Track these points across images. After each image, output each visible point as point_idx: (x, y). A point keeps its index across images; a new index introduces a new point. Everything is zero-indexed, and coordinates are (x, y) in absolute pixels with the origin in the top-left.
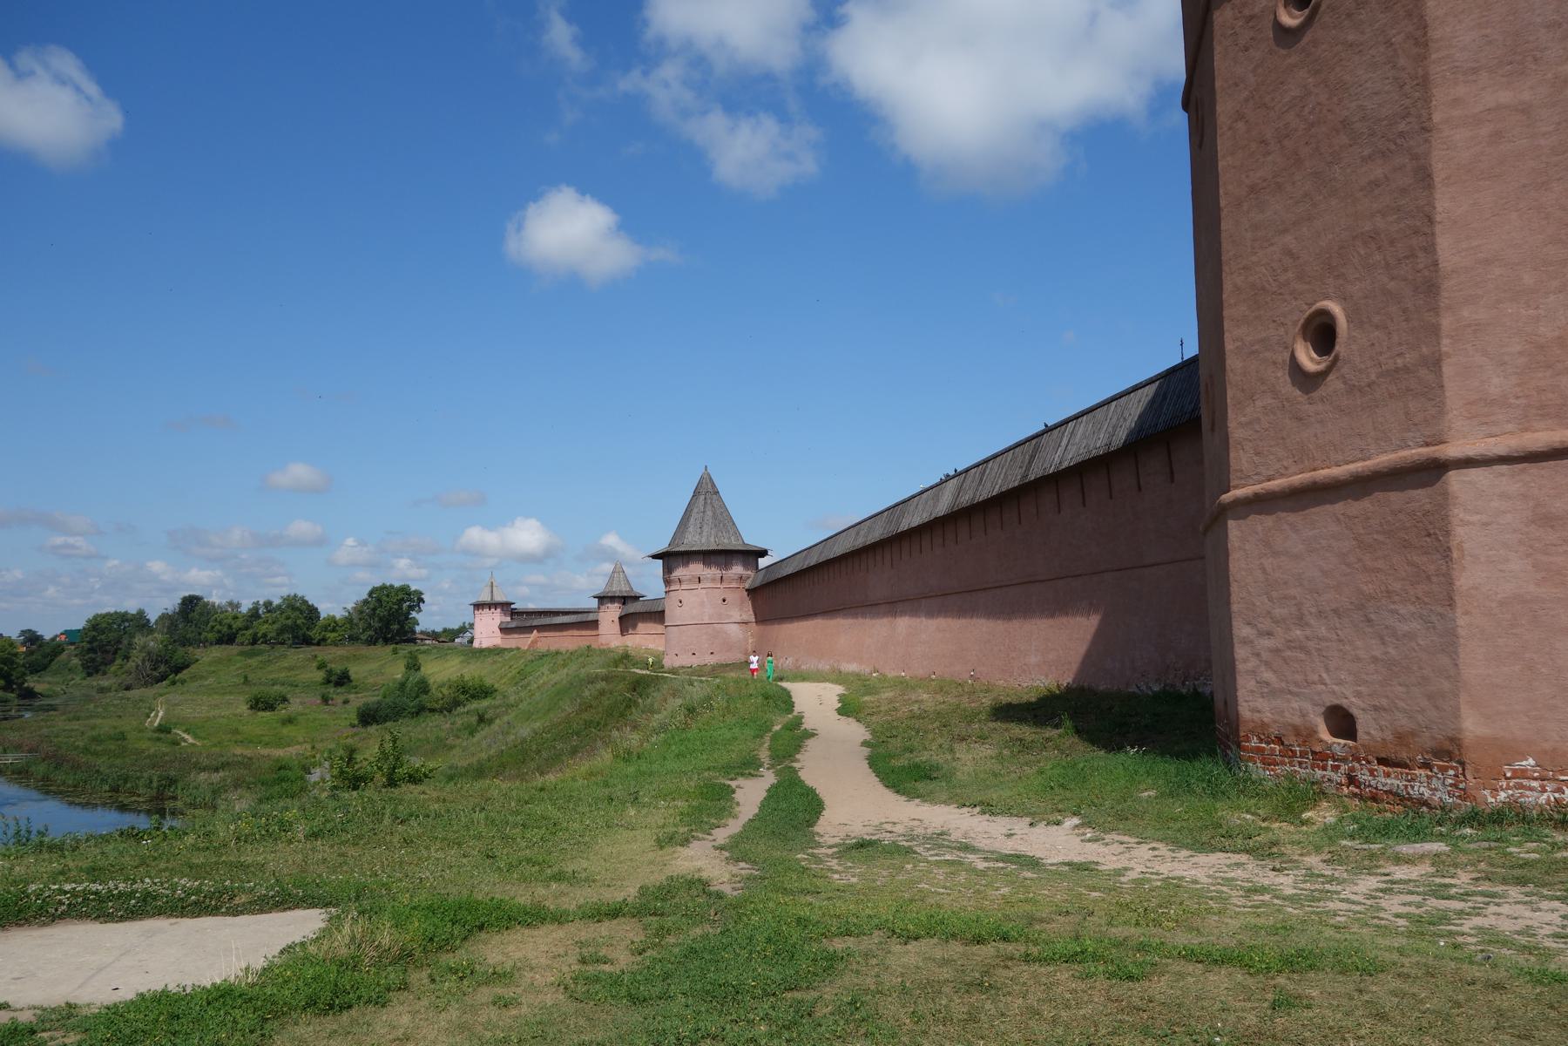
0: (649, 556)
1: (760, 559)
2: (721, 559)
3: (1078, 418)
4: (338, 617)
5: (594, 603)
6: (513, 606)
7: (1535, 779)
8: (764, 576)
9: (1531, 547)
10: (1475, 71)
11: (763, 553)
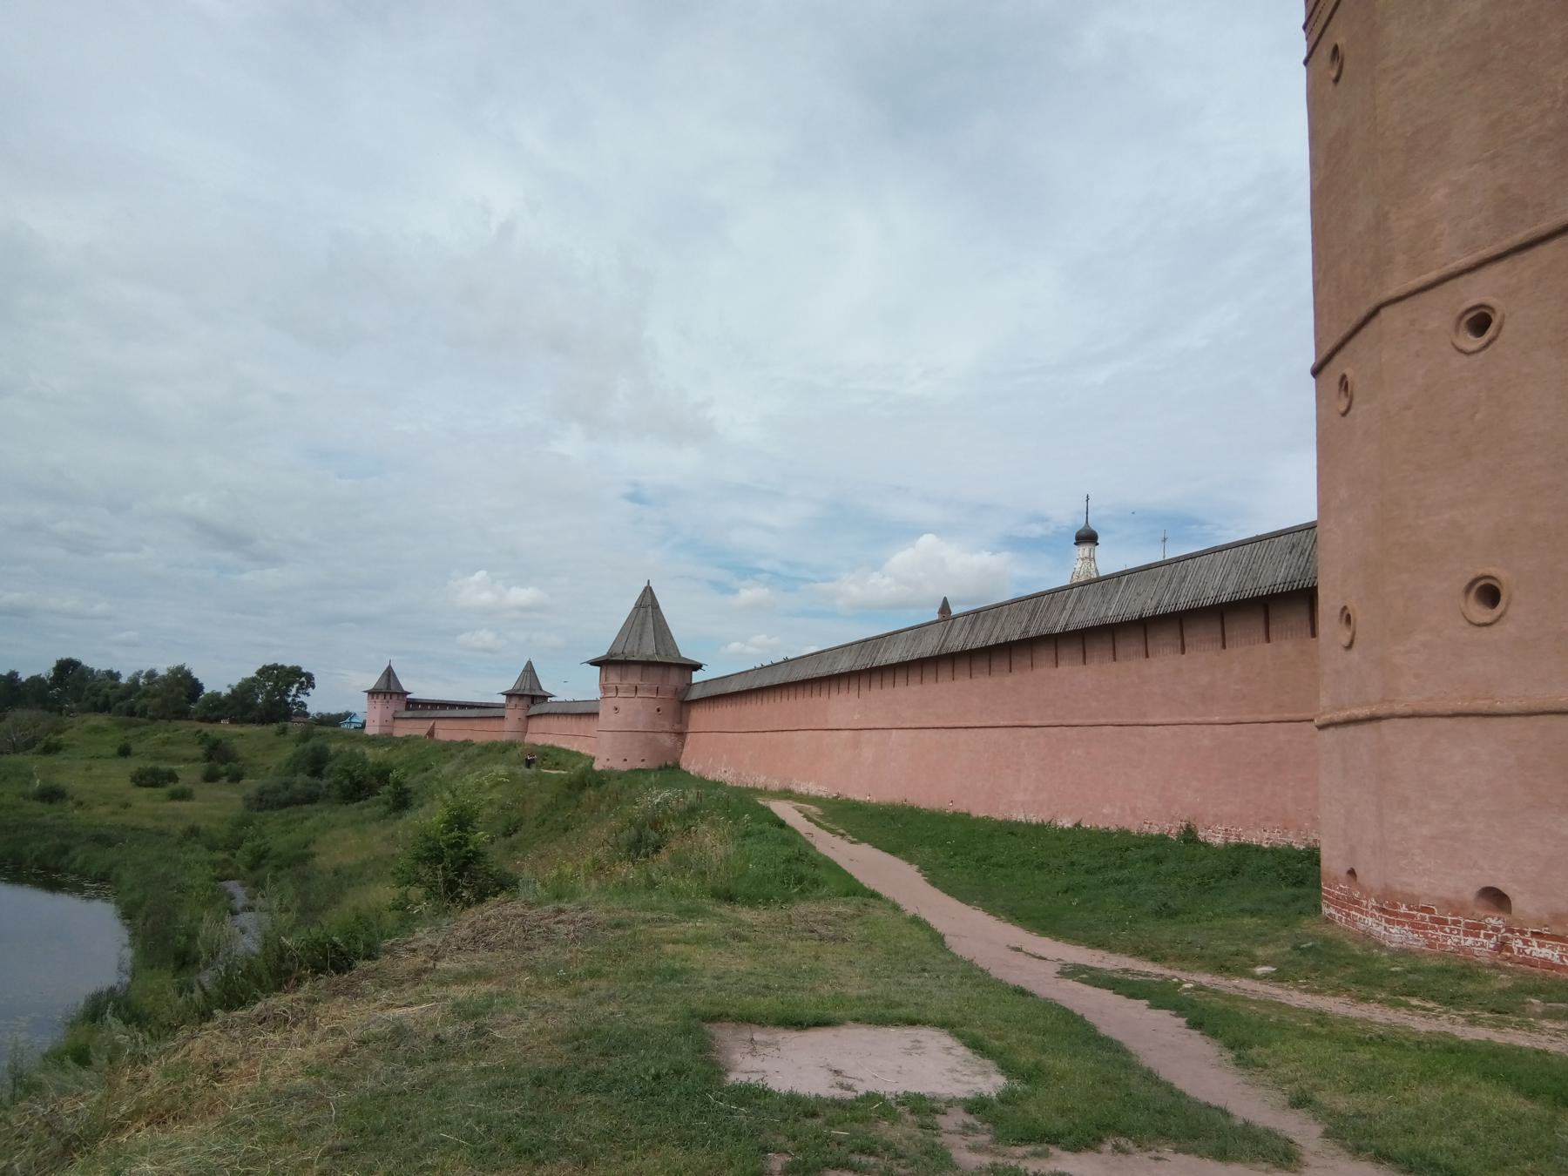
0: (587, 662)
1: (694, 673)
3: (1084, 585)
4: (223, 695)
5: (502, 700)
6: (408, 696)
11: (697, 667)
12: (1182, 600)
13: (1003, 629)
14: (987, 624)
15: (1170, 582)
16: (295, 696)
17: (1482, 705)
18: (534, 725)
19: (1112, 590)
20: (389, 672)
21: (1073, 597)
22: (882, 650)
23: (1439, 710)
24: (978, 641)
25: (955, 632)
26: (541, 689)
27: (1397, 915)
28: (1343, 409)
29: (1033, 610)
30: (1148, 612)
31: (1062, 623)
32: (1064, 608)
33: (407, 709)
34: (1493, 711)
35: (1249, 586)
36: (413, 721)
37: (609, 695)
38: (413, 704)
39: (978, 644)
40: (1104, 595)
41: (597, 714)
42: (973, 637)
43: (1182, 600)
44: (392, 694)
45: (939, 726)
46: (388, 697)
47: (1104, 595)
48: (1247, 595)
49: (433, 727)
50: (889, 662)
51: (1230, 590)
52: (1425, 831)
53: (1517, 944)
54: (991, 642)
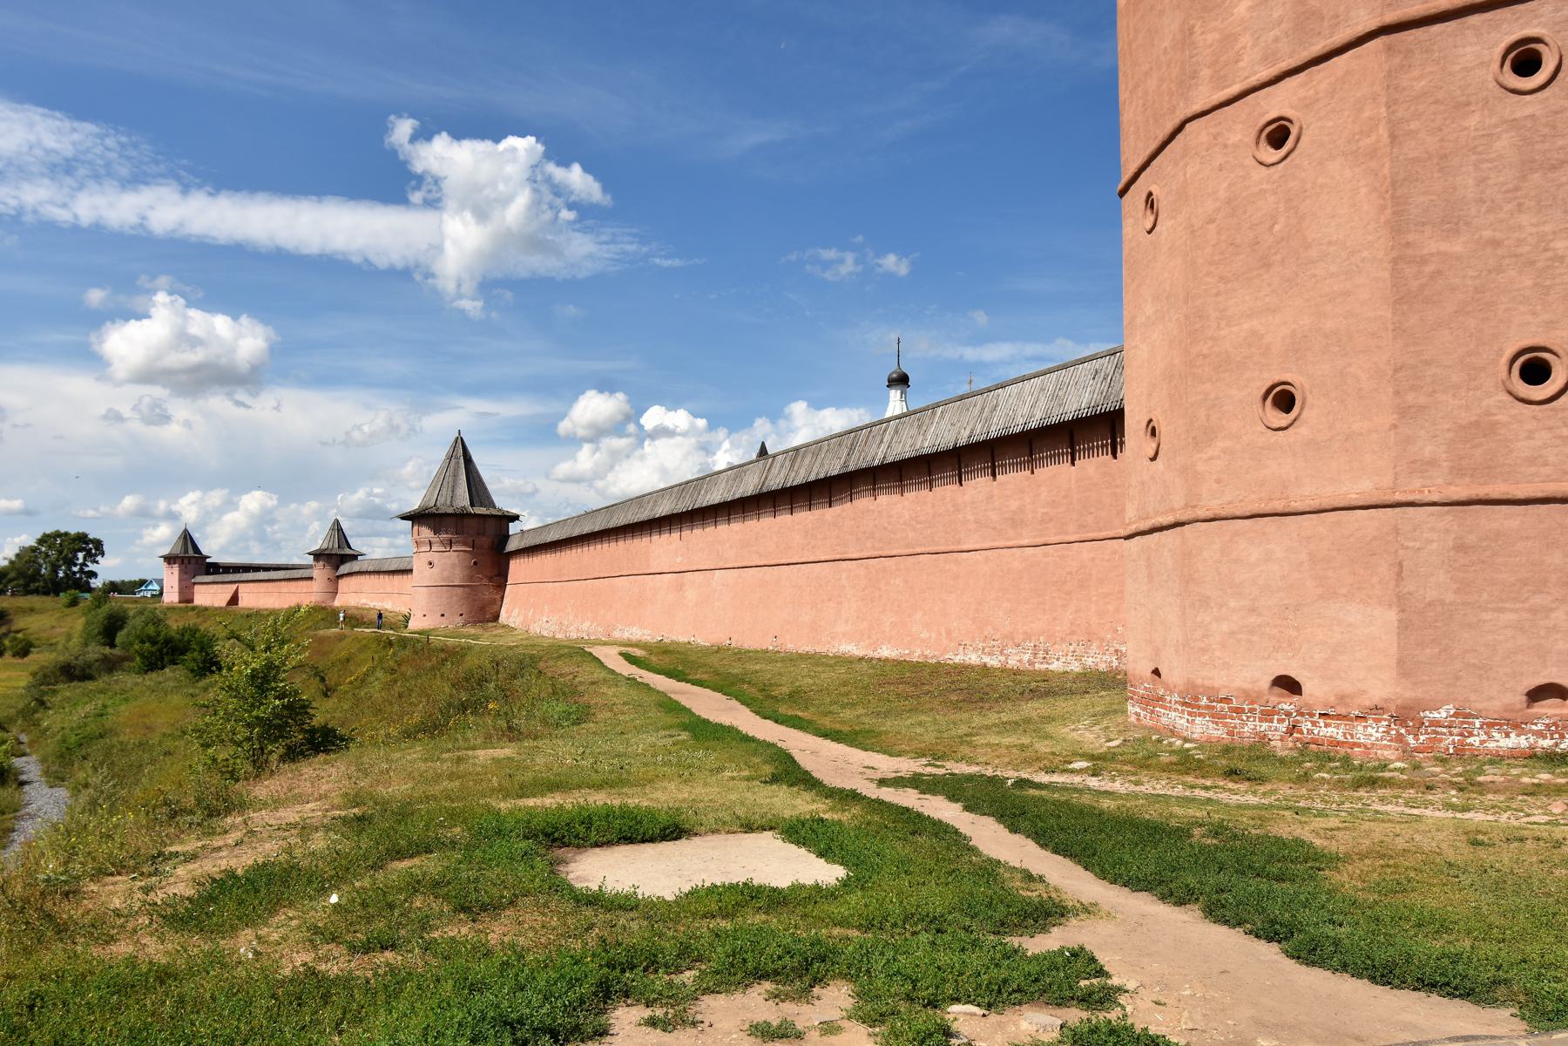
2: (473, 523)
5: (310, 560)
6: (208, 560)
7: (1445, 727)
8: (520, 542)
9: (1451, 566)
10: (1423, 224)
11: (515, 518)
12: (993, 428)
13: (822, 465)
14: (807, 461)
15: (982, 412)
16: (84, 564)
17: (1279, 506)
18: (343, 583)
19: (927, 421)
20: (185, 538)
21: (891, 430)
22: (702, 492)
23: (1238, 513)
24: (800, 477)
25: (775, 471)
26: (350, 547)
27: (1199, 707)
28: (1149, 226)
29: (852, 445)
30: (962, 441)
31: (880, 456)
32: (882, 441)
33: (208, 573)
34: (1287, 510)
35: (1056, 412)
36: (215, 586)
37: (423, 549)
38: (215, 569)
39: (798, 481)
40: (920, 427)
41: (411, 571)
42: (794, 473)
43: (993, 428)
44: (190, 558)
45: (762, 564)
46: (186, 561)
47: (920, 427)
48: (1054, 420)
49: (236, 593)
50: (711, 503)
51: (1038, 417)
52: (1225, 627)
53: (1306, 726)
54: (812, 478)
